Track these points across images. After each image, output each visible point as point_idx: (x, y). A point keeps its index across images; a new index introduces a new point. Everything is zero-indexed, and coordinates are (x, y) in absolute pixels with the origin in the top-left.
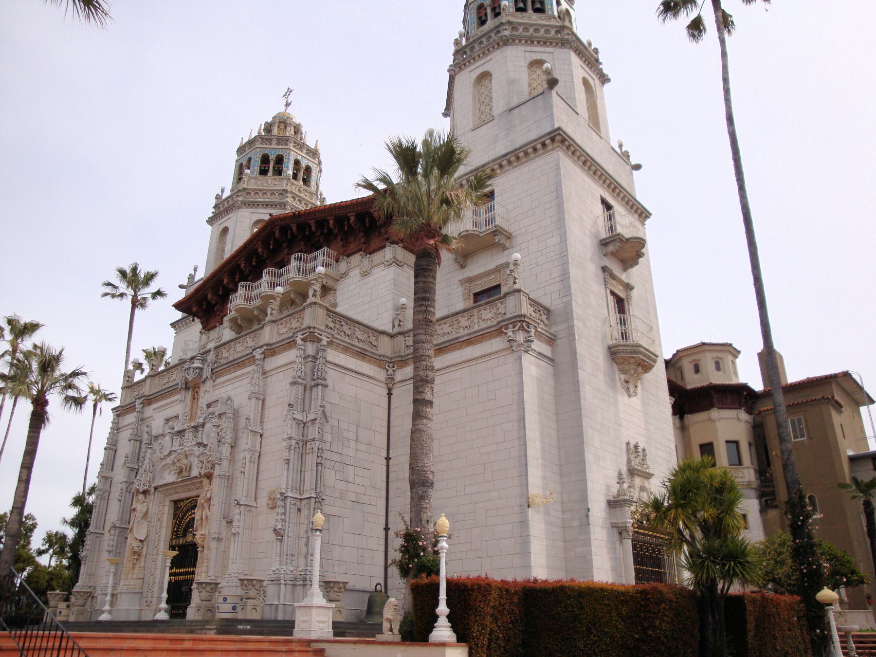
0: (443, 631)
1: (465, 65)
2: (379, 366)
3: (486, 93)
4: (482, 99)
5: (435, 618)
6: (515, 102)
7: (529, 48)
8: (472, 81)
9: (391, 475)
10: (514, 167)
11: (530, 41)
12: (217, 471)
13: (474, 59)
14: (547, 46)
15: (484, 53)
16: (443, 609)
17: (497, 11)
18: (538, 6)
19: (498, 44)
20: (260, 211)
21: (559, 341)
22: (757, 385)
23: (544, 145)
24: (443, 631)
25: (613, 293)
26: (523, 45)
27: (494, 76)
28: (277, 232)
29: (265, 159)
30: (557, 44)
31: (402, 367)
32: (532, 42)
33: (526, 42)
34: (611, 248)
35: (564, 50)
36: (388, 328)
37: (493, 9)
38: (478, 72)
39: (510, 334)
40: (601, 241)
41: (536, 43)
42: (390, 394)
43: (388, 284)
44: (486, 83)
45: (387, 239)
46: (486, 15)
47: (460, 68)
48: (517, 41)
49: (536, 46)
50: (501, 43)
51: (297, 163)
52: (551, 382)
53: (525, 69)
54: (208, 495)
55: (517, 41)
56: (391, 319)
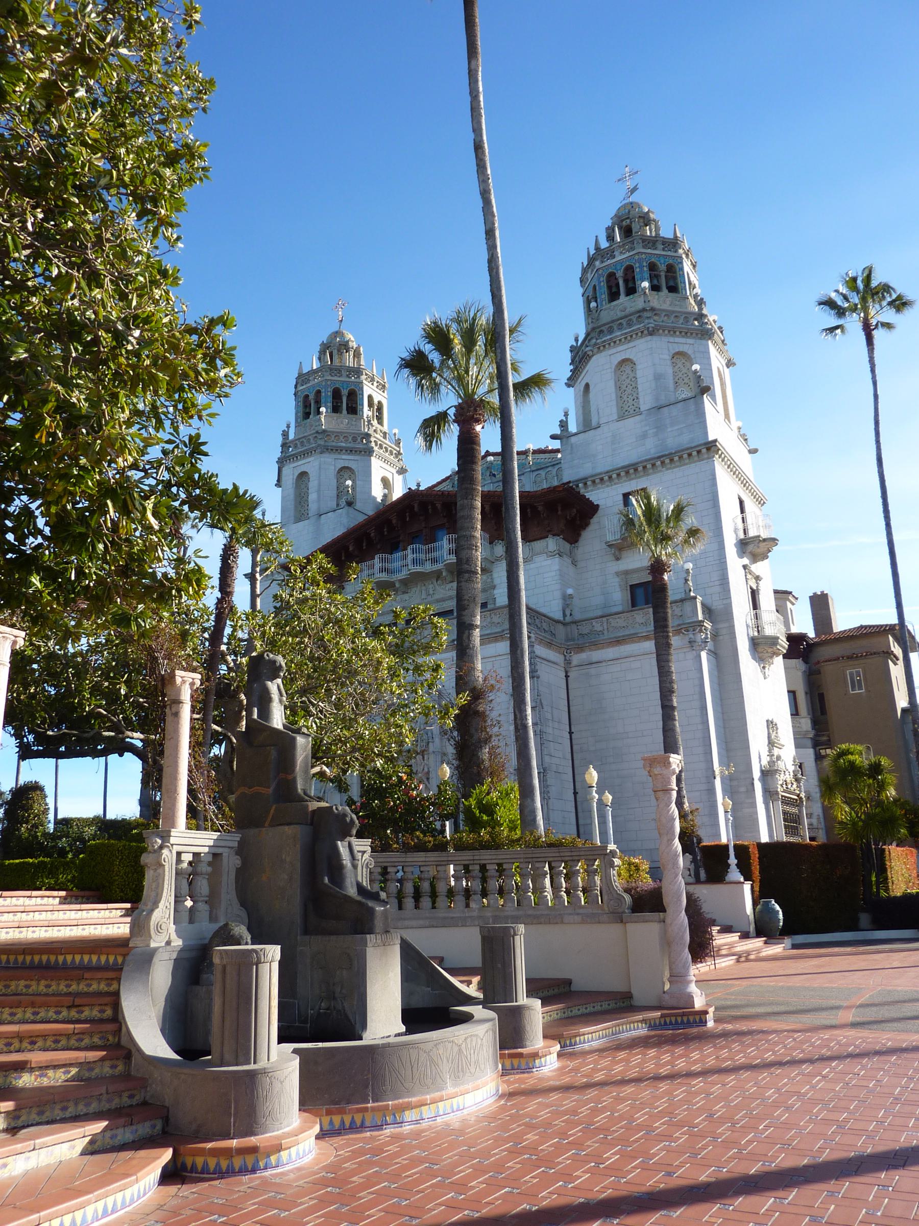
0: (735, 874)
1: (604, 346)
2: (559, 653)
3: (628, 381)
4: (624, 387)
5: (728, 866)
6: (663, 401)
7: (672, 339)
8: (614, 367)
9: (575, 747)
10: (668, 469)
11: (672, 331)
12: (431, 748)
13: (615, 342)
14: (688, 337)
15: (626, 338)
16: (733, 861)
17: (631, 285)
18: (671, 283)
19: (642, 332)
20: (344, 457)
21: (721, 638)
22: (811, 634)
23: (699, 452)
24: (735, 874)
25: (751, 588)
26: (666, 335)
27: (638, 367)
28: (416, 506)
29: (337, 394)
30: (697, 334)
31: (577, 653)
32: (675, 332)
33: (669, 331)
34: (750, 548)
35: (703, 342)
36: (558, 616)
37: (626, 281)
38: (619, 357)
39: (691, 636)
40: (741, 540)
41: (678, 333)
42: (567, 676)
43: (554, 574)
44: (627, 368)
45: (549, 531)
46: (618, 285)
47: (599, 348)
48: (661, 331)
49: (678, 336)
50: (646, 332)
51: (370, 397)
52: (716, 673)
53: (669, 363)
54: (426, 770)
55: (661, 331)
56: (561, 608)
